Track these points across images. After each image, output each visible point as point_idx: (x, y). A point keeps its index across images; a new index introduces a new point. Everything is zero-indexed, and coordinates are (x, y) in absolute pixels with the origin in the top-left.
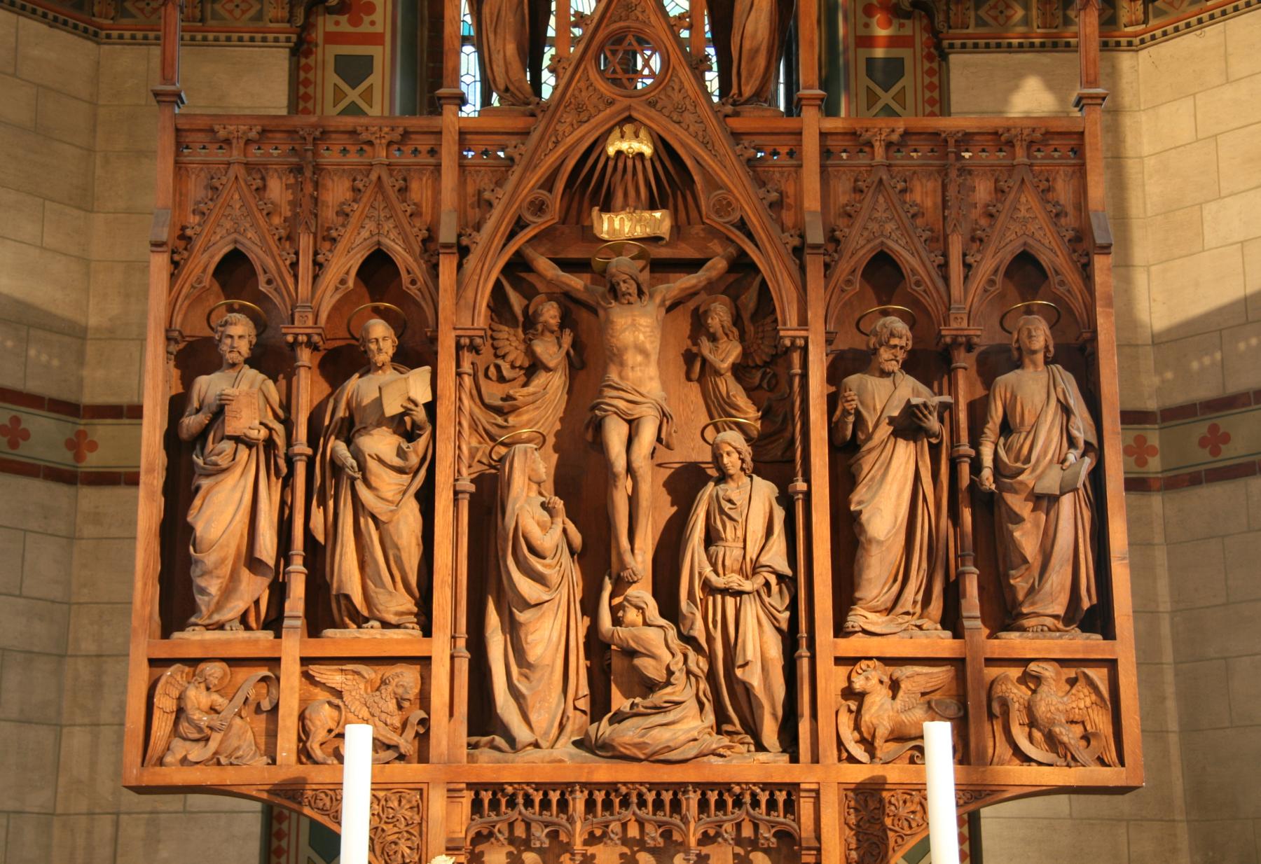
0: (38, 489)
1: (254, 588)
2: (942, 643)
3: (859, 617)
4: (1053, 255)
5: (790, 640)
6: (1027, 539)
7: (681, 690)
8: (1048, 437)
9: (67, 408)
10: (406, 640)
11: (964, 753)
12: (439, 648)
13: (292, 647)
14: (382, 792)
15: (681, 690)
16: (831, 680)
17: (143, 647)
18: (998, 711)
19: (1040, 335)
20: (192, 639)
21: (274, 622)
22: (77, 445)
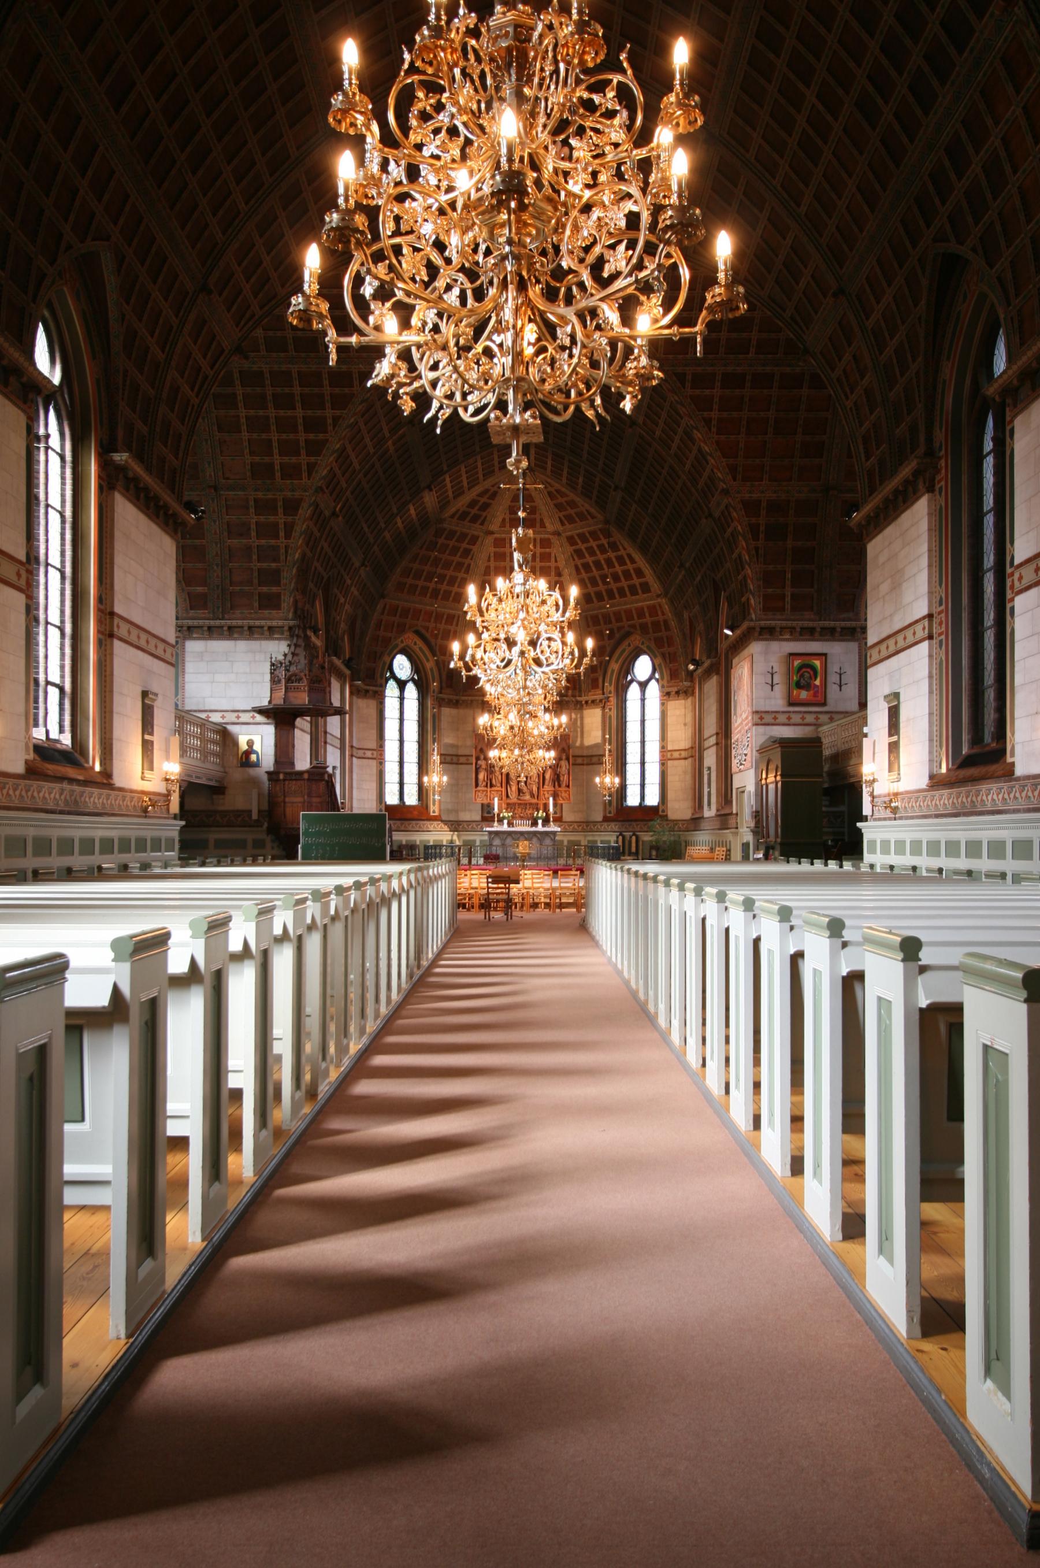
0: (454, 766)
1: (484, 784)
2: (553, 789)
3: (545, 786)
4: (566, 748)
5: (538, 788)
6: (562, 779)
7: (527, 794)
8: (564, 768)
9: (457, 756)
10: (500, 789)
11: (554, 799)
12: (504, 790)
13: (489, 789)
14: (499, 804)
15: (527, 794)
16: (542, 792)
17: (474, 789)
18: (558, 795)
19: (564, 757)
20: (479, 788)
21: (487, 786)
22: (458, 760)
